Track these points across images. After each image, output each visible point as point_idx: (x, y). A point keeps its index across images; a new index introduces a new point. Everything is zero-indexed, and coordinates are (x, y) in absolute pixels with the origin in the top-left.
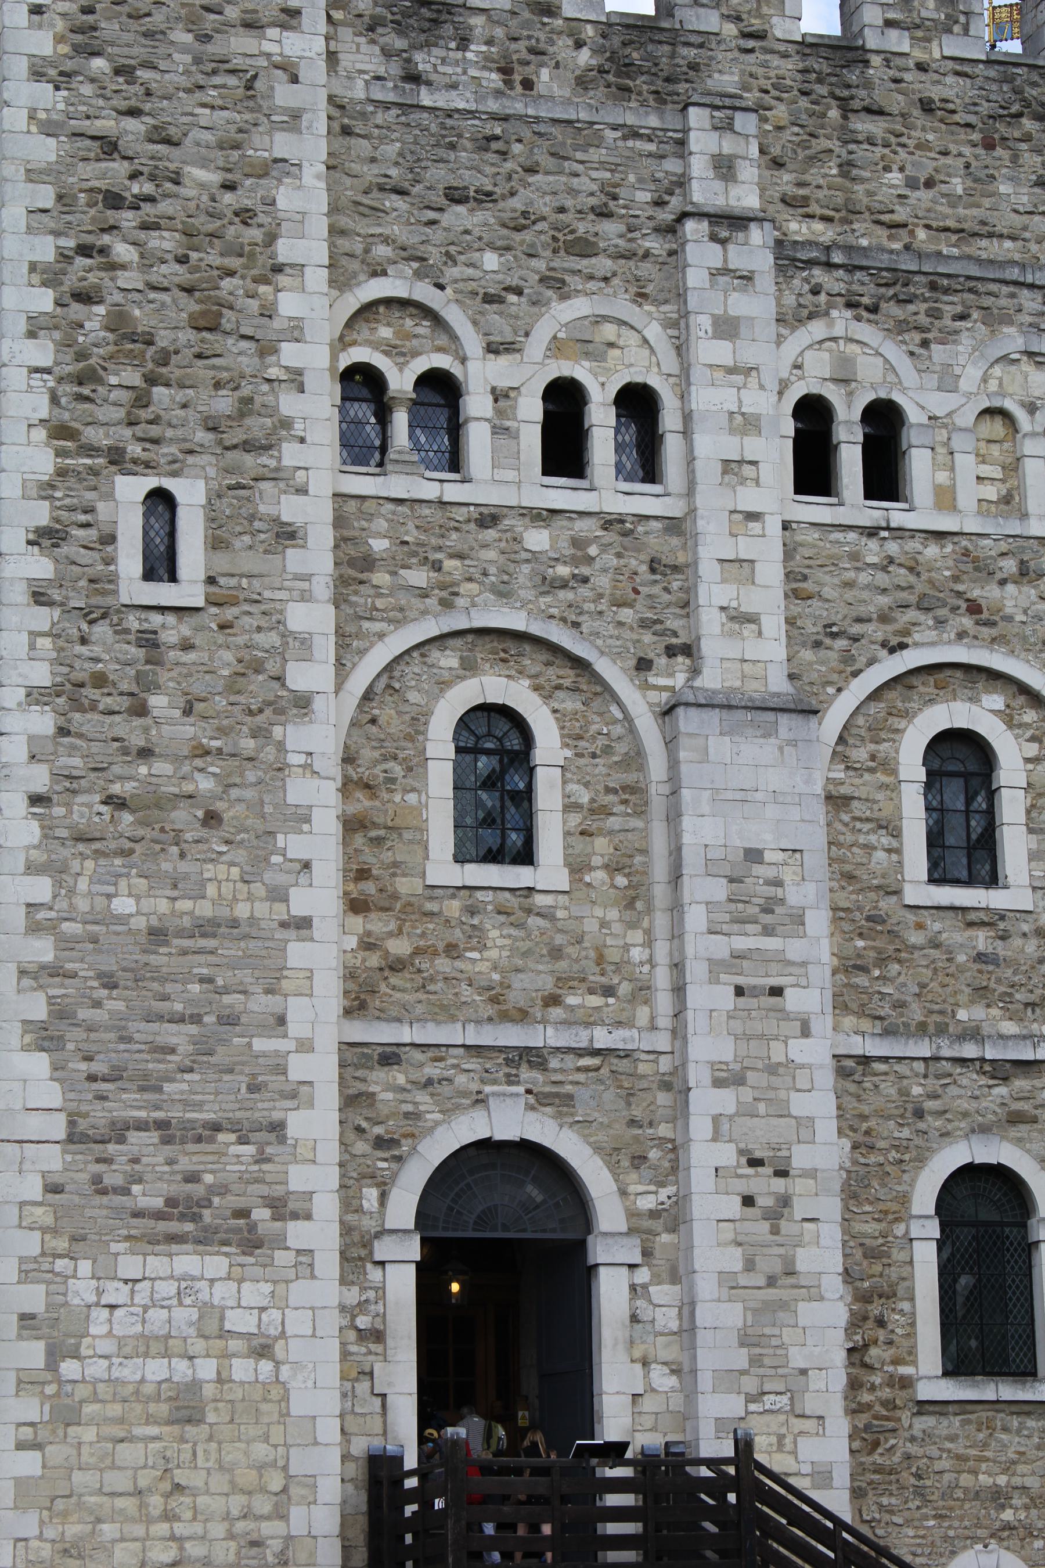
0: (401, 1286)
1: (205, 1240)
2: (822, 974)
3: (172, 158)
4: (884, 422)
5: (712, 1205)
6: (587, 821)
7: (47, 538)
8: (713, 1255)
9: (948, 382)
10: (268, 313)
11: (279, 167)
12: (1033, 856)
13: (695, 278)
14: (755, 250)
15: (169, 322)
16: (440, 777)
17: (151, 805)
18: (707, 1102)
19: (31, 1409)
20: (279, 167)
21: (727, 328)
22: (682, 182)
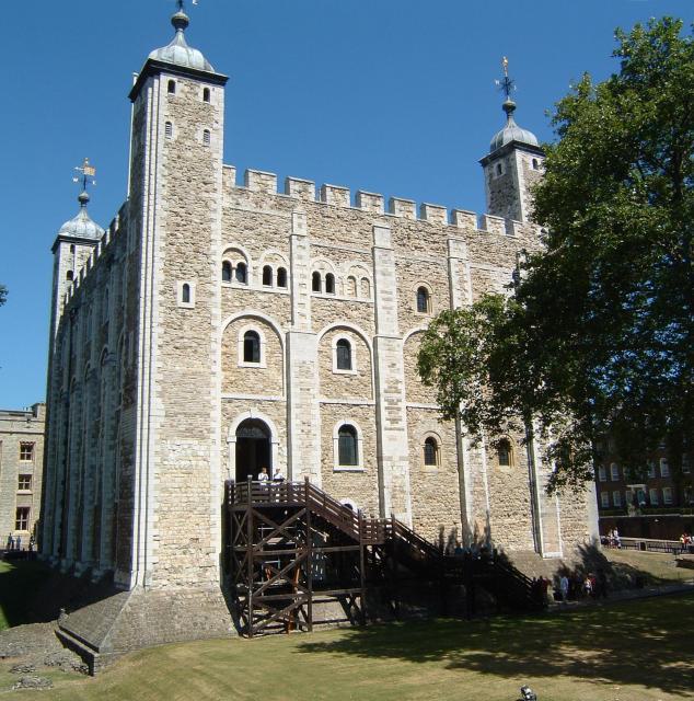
0: (233, 447)
1: (194, 437)
2: (318, 386)
3: (190, 217)
4: (330, 278)
5: (295, 431)
7: (163, 293)
8: (295, 442)
9: (343, 270)
10: (209, 249)
11: (211, 220)
12: (358, 364)
15: (189, 250)
16: (241, 346)
18: (294, 411)
19: (157, 470)
20: (211, 220)
21: (300, 257)
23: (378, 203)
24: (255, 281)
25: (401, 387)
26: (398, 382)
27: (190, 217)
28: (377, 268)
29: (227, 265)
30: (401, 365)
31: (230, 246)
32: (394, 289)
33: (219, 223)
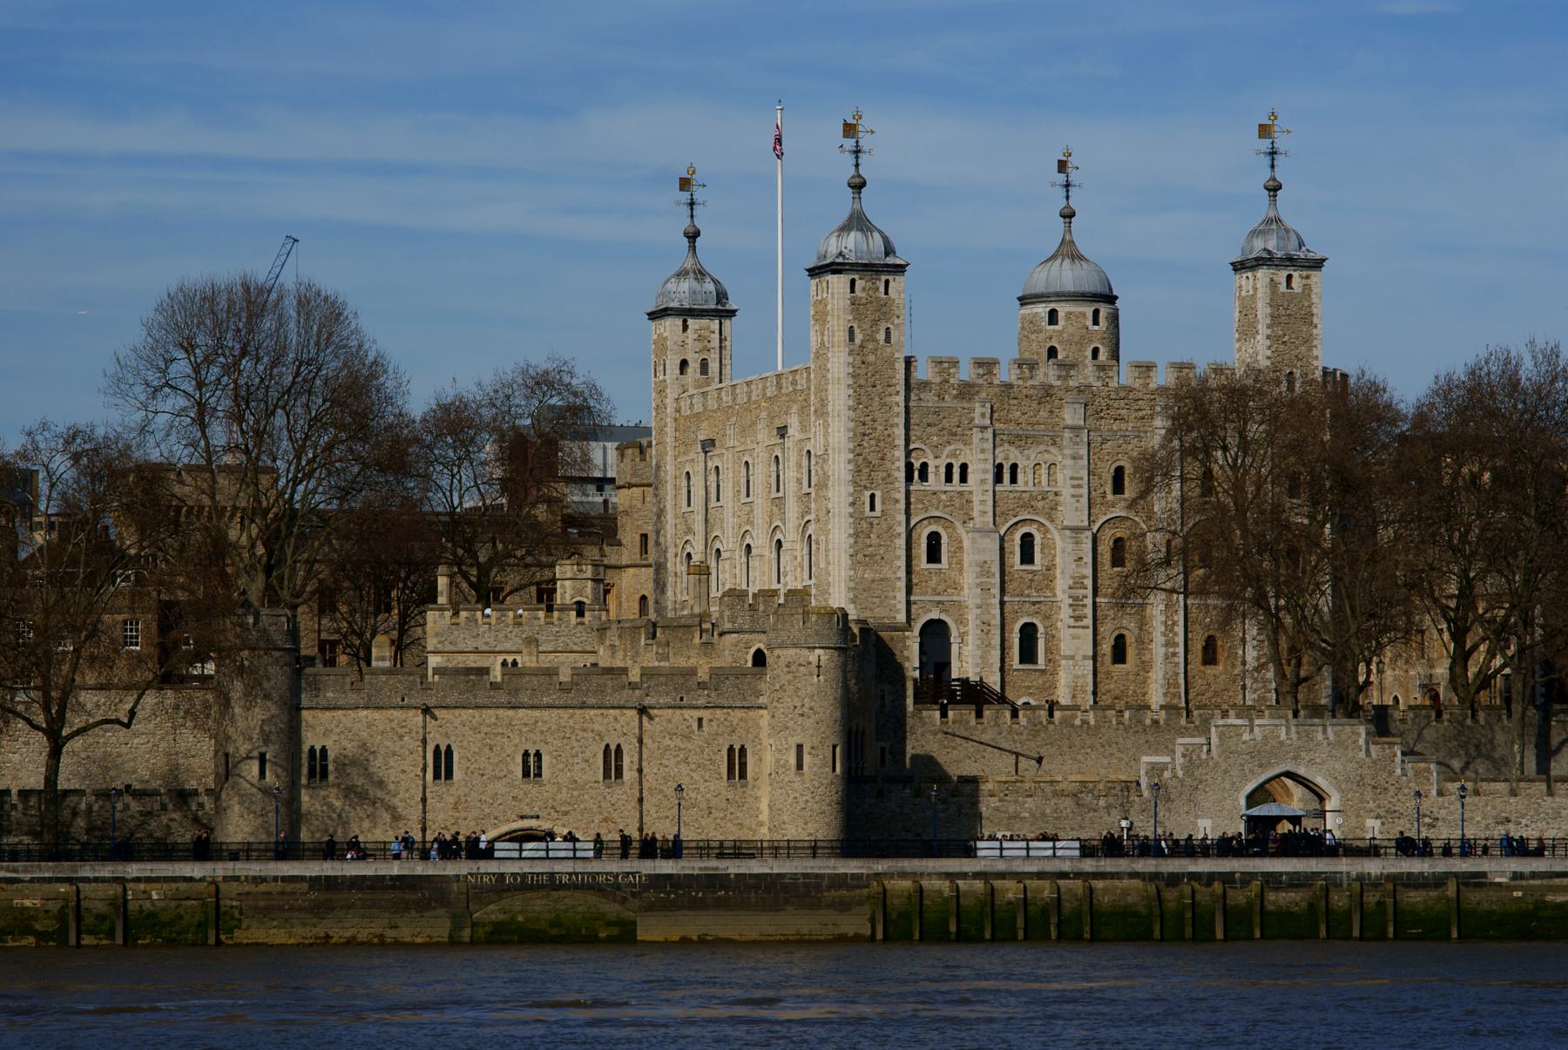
4: (1014, 467)
6: (952, 554)
13: (975, 440)
14: (989, 434)
16: (924, 547)
21: (983, 451)
22: (973, 419)
24: (935, 481)
25: (1089, 582)
26: (1084, 577)
28: (1067, 452)
29: (909, 467)
30: (1088, 559)
32: (1085, 473)
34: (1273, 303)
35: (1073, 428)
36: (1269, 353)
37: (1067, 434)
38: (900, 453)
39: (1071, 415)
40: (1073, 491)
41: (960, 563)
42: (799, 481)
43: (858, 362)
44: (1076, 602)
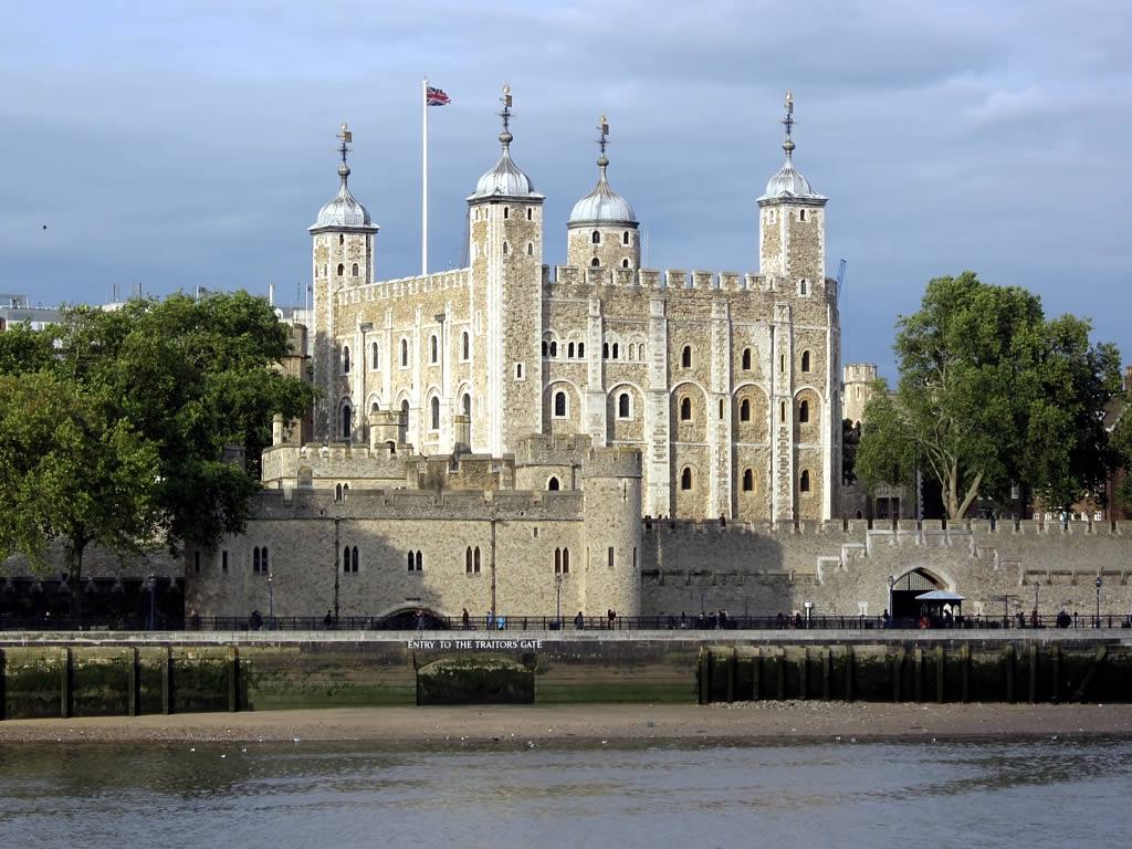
4: (616, 346)
7: (506, 371)
13: (589, 326)
14: (600, 321)
17: (519, 410)
21: (595, 334)
23: (655, 278)
24: (561, 355)
25: (667, 430)
27: (522, 314)
31: (546, 330)
33: (540, 314)
34: (792, 230)
35: (656, 318)
36: (789, 266)
37: (652, 323)
38: (538, 335)
39: (655, 309)
40: (656, 364)
41: (578, 415)
42: (455, 355)
43: (510, 269)
44: (658, 445)
